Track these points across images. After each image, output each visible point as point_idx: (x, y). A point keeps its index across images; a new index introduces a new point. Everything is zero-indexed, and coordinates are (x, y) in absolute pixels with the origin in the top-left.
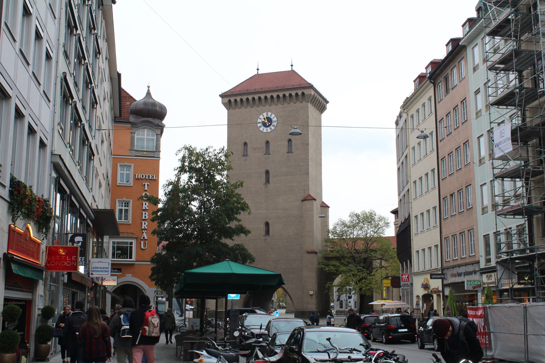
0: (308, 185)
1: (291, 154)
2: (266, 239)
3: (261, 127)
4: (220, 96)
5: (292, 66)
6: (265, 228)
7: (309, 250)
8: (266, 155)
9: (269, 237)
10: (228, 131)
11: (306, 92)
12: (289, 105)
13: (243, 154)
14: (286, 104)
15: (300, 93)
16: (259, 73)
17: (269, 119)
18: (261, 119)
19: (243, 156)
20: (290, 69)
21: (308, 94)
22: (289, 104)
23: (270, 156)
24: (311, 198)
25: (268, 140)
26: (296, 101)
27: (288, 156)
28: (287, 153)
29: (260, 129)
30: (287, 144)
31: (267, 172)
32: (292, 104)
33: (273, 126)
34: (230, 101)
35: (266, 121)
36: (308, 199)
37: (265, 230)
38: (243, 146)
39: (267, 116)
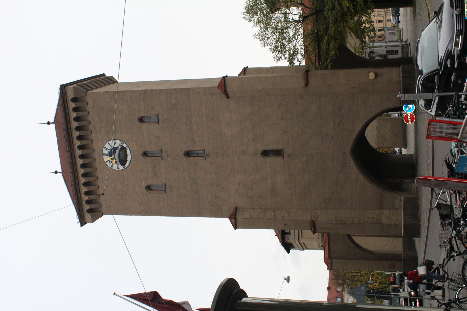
0: (205, 88)
1: (160, 117)
2: (289, 155)
5: (49, 123)
6: (272, 157)
7: (303, 83)
8: (163, 156)
9: (285, 150)
10: (131, 215)
11: (70, 94)
12: (92, 122)
13: (164, 191)
14: (91, 127)
15: (72, 105)
17: (112, 151)
18: (113, 165)
19: (166, 192)
20: (53, 126)
21: (74, 93)
22: (90, 122)
24: (223, 82)
25: (141, 152)
26: (85, 111)
27: (164, 122)
28: (159, 123)
30: (145, 123)
31: (188, 154)
32: (90, 118)
34: (89, 211)
36: (223, 87)
37: (275, 157)
38: (152, 192)
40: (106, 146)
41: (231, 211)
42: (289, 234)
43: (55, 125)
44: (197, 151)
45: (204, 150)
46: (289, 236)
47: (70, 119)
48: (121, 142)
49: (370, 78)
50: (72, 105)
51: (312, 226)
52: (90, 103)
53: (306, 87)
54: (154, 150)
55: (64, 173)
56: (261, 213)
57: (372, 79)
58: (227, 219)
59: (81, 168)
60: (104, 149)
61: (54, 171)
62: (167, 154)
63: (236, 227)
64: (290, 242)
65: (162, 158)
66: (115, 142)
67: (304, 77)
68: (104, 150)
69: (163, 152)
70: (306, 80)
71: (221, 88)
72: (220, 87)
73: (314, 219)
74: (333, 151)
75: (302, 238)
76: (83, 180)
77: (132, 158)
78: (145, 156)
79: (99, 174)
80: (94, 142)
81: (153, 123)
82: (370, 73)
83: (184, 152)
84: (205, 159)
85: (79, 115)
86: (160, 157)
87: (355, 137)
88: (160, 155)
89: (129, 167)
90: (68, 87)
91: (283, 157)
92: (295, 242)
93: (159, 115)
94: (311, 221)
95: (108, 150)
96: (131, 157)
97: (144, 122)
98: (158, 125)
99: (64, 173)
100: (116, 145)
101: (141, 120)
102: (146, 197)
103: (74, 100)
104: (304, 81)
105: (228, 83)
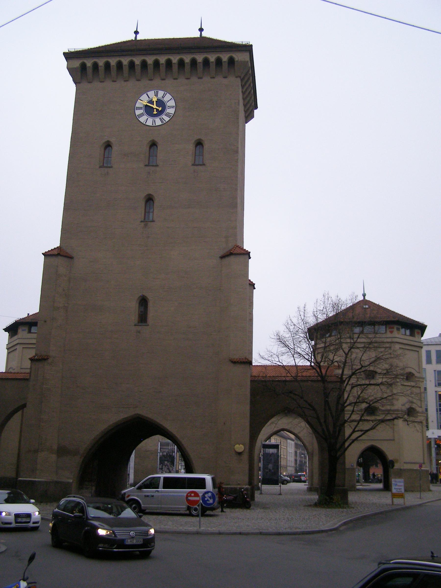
1: (201, 168)
3: (142, 115)
4: (64, 54)
5: (201, 30)
7: (236, 357)
11: (239, 57)
12: (200, 80)
13: (102, 164)
14: (194, 79)
15: (225, 57)
17: (160, 103)
20: (197, 34)
23: (158, 169)
24: (243, 252)
27: (194, 171)
29: (140, 119)
31: (149, 199)
32: (206, 79)
33: (168, 115)
34: (83, 67)
36: (235, 252)
37: (137, 313)
40: (168, 94)
42: (30, 332)
43: (198, 38)
44: (153, 212)
45: (153, 221)
46: (27, 331)
47: (207, 53)
48: (172, 115)
49: (237, 445)
50: (225, 57)
51: (40, 356)
52: (225, 81)
53: (230, 360)
54: (158, 155)
55: (135, 42)
56: (64, 290)
58: (59, 245)
59: (142, 60)
60: (164, 93)
61: (138, 30)
62: (151, 172)
63: (46, 255)
66: (172, 108)
67: (243, 359)
68: (163, 92)
70: (239, 362)
71: (234, 248)
72: (236, 248)
73: (50, 360)
74: (141, 392)
75: (23, 348)
76: (125, 61)
77: (151, 128)
78: (151, 143)
79: (132, 83)
80: (175, 81)
81: (194, 158)
82: (244, 446)
83: (153, 194)
84: (141, 222)
85: (211, 64)
87: (158, 422)
88: (151, 164)
89: (139, 122)
90: (248, 54)
91: (137, 324)
92: (19, 339)
93: (203, 166)
94: (48, 356)
95: (163, 97)
96: (151, 125)
97: (196, 146)
98: (191, 164)
99: (134, 42)
101: (199, 144)
102: (96, 140)
104: (238, 359)
105: (242, 258)
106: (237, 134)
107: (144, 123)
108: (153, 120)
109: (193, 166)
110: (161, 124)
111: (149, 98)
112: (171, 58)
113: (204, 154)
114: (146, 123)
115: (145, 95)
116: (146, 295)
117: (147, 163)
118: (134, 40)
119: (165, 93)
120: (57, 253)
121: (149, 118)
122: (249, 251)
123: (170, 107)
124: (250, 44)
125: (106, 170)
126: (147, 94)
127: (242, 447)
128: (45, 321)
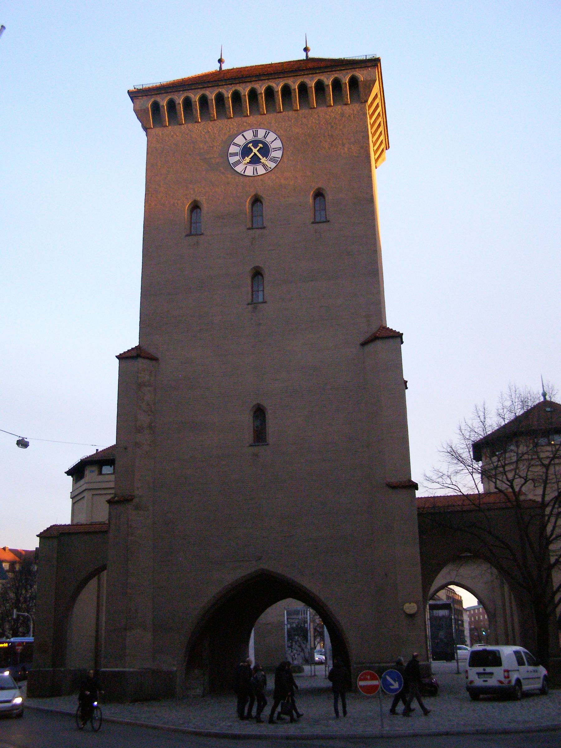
2: (256, 455)
5: (306, 50)
7: (394, 480)
16: (223, 68)
19: (187, 236)
20: (302, 56)
23: (265, 232)
25: (260, 193)
28: (313, 223)
31: (257, 273)
34: (156, 107)
35: (255, 150)
39: (256, 139)
40: (271, 133)
41: (152, 351)
42: (100, 473)
43: (303, 60)
44: (263, 291)
45: (264, 302)
49: (407, 605)
56: (148, 405)
57: (406, 609)
58: (137, 344)
60: (266, 131)
63: (121, 357)
64: (85, 473)
65: (249, 229)
66: (278, 150)
68: (264, 131)
69: (259, 232)
70: (400, 486)
75: (93, 495)
84: (248, 304)
86: (252, 226)
88: (255, 226)
93: (328, 223)
95: (265, 137)
96: (252, 175)
100: (273, 151)
103: (354, 82)
105: (391, 342)
106: (369, 177)
107: (242, 173)
108: (254, 168)
109: (314, 225)
110: (265, 172)
111: (246, 140)
112: (272, 84)
113: (327, 207)
114: (244, 173)
115: (240, 136)
116: (262, 403)
117: (249, 225)
118: (219, 70)
119: (267, 132)
120: (135, 355)
121: (248, 166)
122: (401, 332)
123: (276, 149)
124: (377, 57)
125: (195, 239)
126: (243, 135)
127: (413, 606)
128: (126, 449)
